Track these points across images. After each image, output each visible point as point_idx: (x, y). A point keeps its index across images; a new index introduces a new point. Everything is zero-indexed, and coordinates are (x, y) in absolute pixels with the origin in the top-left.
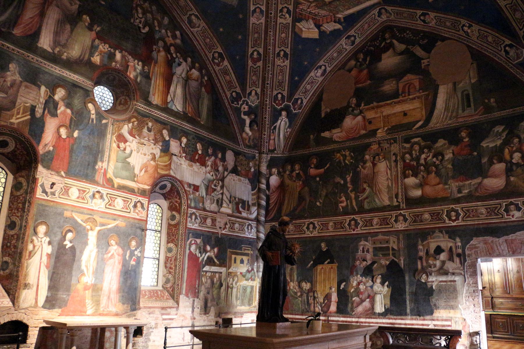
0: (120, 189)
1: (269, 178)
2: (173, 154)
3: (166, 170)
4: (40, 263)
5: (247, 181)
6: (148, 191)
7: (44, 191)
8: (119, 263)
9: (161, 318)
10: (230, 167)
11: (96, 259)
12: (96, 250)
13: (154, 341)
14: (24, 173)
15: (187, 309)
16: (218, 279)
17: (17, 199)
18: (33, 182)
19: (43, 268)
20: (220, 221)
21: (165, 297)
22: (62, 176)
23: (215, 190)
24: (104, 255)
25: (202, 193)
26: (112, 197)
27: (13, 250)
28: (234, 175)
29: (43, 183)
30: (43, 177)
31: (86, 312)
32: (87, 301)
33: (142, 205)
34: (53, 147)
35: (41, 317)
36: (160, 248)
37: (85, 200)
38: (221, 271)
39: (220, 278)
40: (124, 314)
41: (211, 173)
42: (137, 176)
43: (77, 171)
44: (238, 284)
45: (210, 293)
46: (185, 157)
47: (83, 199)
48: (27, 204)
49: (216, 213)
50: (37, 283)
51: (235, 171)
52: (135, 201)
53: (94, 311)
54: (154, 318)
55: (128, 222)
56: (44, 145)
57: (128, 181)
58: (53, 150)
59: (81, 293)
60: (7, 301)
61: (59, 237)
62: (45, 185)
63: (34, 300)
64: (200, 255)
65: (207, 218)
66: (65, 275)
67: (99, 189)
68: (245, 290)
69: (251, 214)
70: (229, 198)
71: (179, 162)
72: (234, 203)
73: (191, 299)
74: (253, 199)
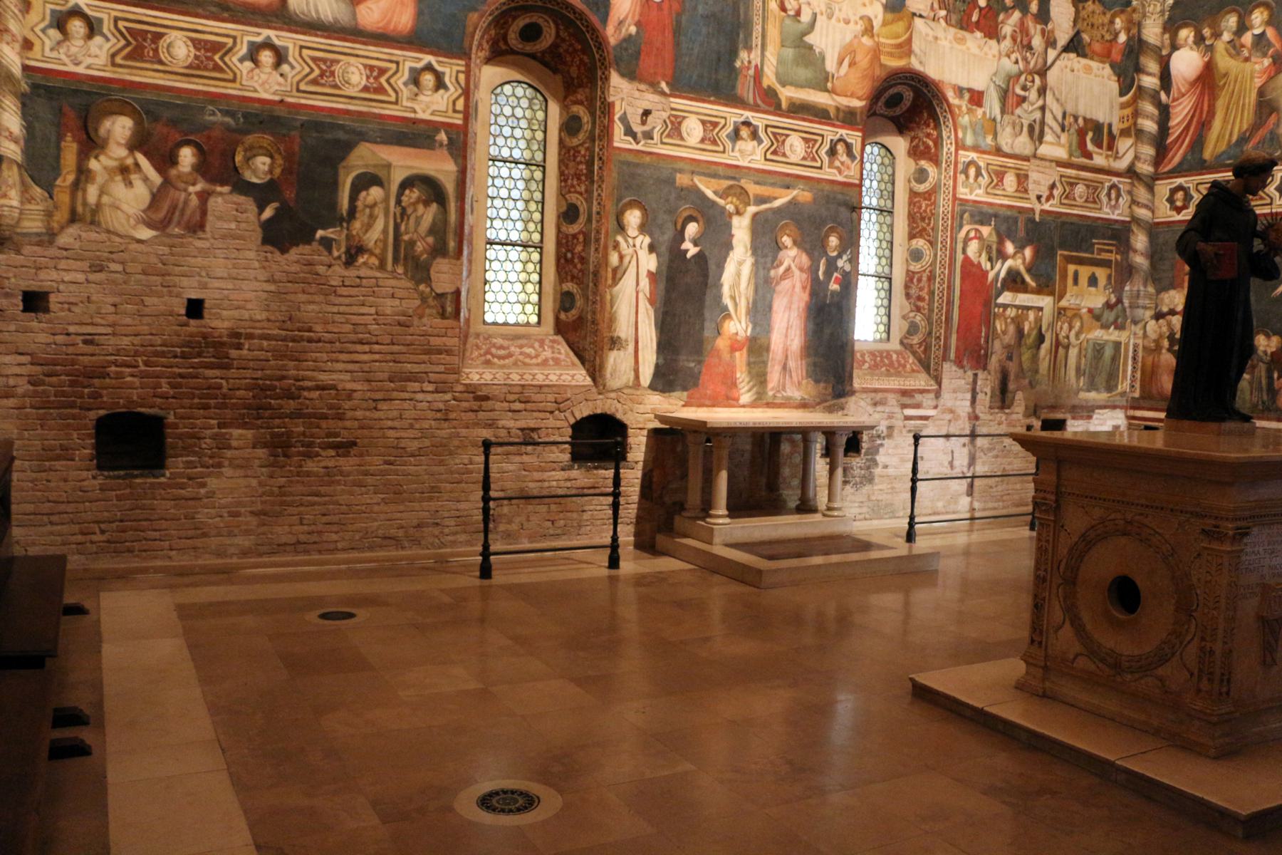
1: (1169, 55)
2: (914, 14)
3: (901, 58)
4: (637, 293)
5: (1107, 70)
6: (862, 113)
7: (629, 132)
8: (804, 288)
9: (900, 416)
10: (1063, 38)
11: (753, 281)
12: (749, 261)
13: (886, 467)
14: (580, 96)
15: (960, 395)
16: (1033, 325)
17: (574, 155)
18: (602, 112)
19: (644, 306)
20: (1040, 179)
21: (908, 366)
22: (663, 93)
23: (1024, 99)
24: (769, 270)
25: (991, 108)
27: (579, 266)
28: (1073, 55)
29: (625, 113)
30: (622, 99)
31: (737, 400)
32: (738, 375)
33: (849, 147)
34: (636, 25)
35: (648, 408)
36: (891, 251)
37: (718, 145)
38: (1040, 304)
39: (1038, 320)
40: (819, 404)
41: (1013, 57)
42: (833, 77)
43: (695, 77)
44: (1082, 337)
45: (1014, 358)
46: (946, 19)
47: (714, 142)
48: (596, 163)
49: (1026, 159)
51: (1075, 46)
52: (832, 140)
53: (755, 397)
54: (885, 415)
56: (616, 24)
57: (812, 91)
58: (638, 32)
59: (726, 356)
61: (668, 235)
63: (633, 373)
64: (989, 265)
65: (1006, 172)
67: (748, 115)
68: (1098, 351)
69: (1116, 158)
70: (1060, 118)
71: (931, 33)
72: (1072, 130)
73: (970, 373)
74: (1122, 119)
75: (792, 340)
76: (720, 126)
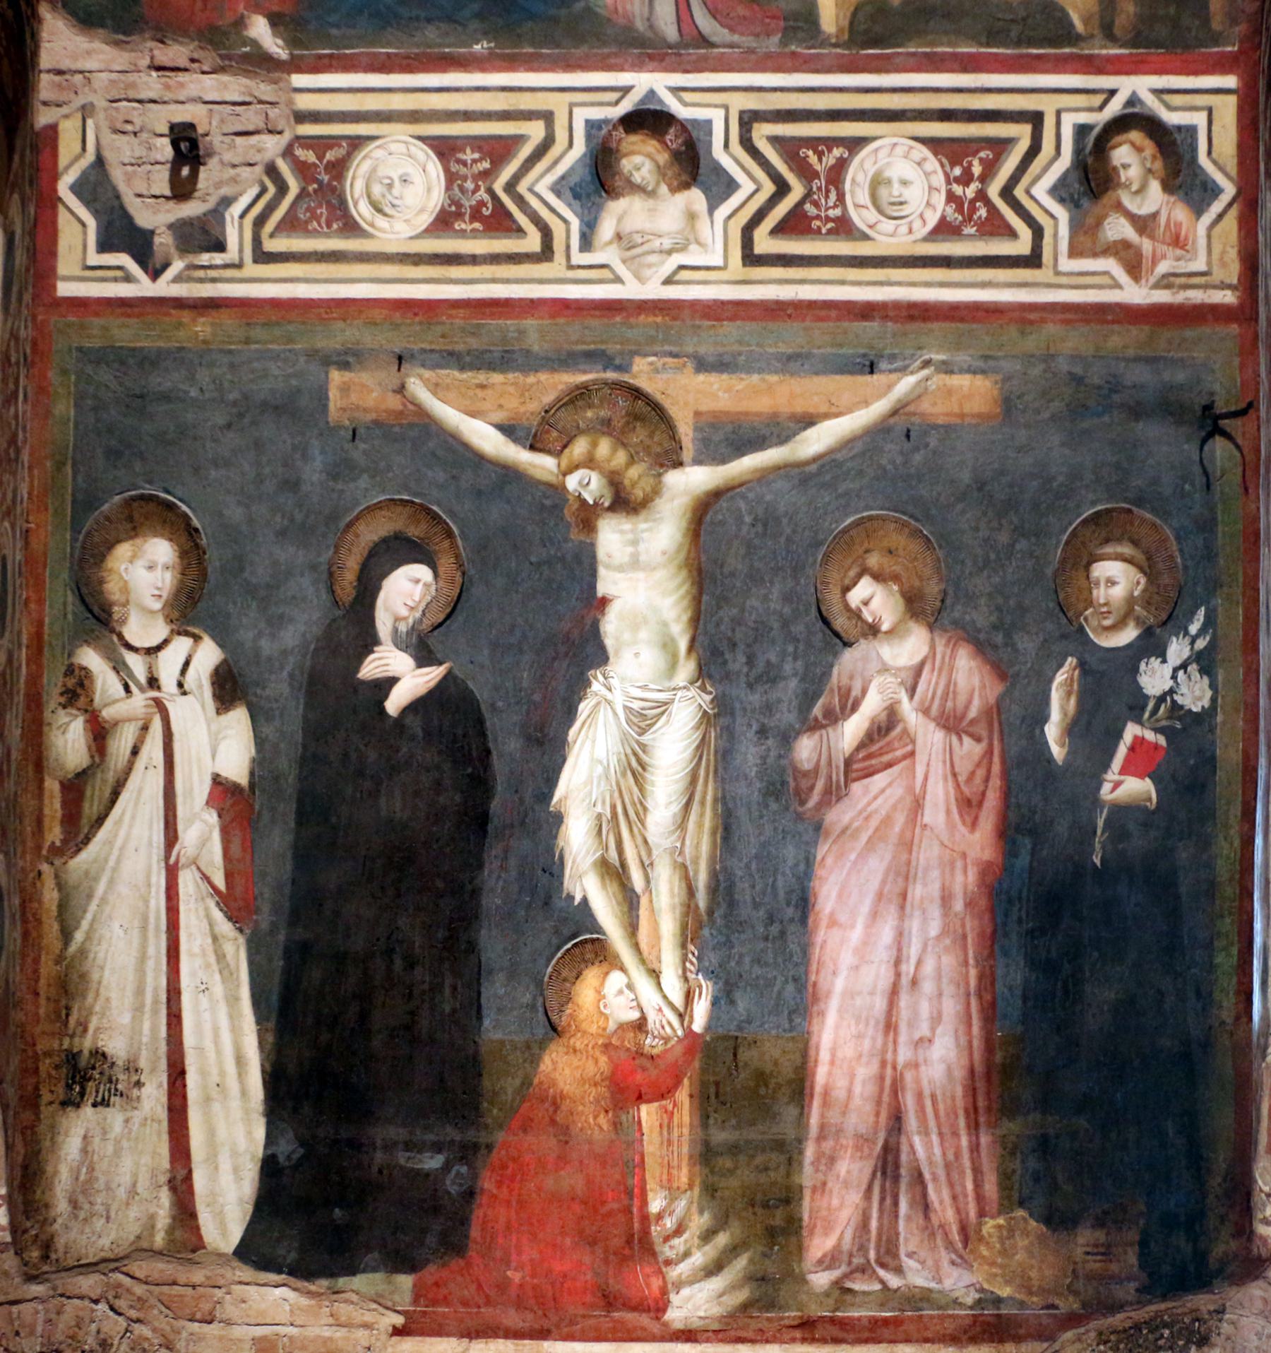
0: (875, 43)
8: (969, 805)
26: (813, 142)
47: (499, 222)
50: (163, 1048)
55: (1029, 358)
62: (117, 175)
66: (411, 964)
75: (922, 1043)
76: (526, 151)
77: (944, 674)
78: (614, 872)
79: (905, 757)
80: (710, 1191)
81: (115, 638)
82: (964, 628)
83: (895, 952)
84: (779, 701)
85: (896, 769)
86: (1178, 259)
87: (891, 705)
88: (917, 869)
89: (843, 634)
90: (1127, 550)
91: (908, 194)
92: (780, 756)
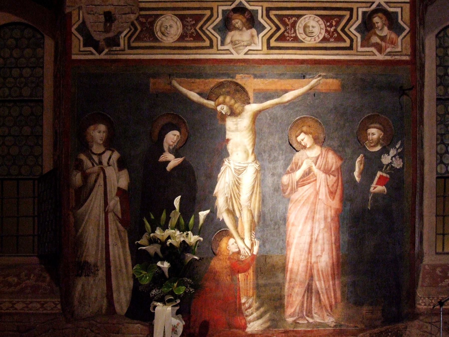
24: (280, 176)
26: (287, 16)
31: (245, 327)
37: (204, 41)
52: (364, 13)
60: (53, 302)
77: (325, 159)
78: (232, 212)
79: (314, 181)
80: (258, 297)
81: (90, 152)
82: (330, 147)
83: (311, 233)
84: (278, 166)
85: (311, 184)
86: (393, 48)
87: (310, 167)
88: (317, 210)
89: (296, 148)
90: (377, 125)
91: (314, 30)
92: (278, 181)
